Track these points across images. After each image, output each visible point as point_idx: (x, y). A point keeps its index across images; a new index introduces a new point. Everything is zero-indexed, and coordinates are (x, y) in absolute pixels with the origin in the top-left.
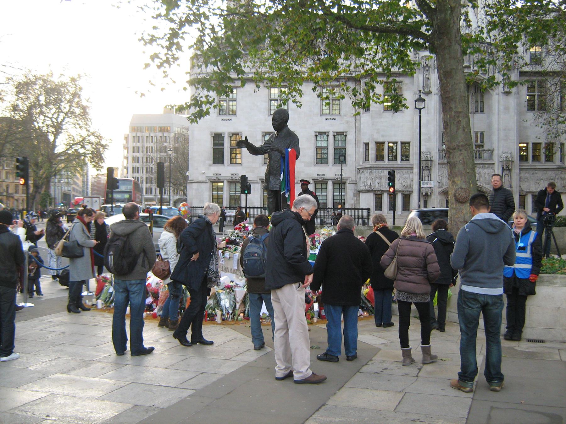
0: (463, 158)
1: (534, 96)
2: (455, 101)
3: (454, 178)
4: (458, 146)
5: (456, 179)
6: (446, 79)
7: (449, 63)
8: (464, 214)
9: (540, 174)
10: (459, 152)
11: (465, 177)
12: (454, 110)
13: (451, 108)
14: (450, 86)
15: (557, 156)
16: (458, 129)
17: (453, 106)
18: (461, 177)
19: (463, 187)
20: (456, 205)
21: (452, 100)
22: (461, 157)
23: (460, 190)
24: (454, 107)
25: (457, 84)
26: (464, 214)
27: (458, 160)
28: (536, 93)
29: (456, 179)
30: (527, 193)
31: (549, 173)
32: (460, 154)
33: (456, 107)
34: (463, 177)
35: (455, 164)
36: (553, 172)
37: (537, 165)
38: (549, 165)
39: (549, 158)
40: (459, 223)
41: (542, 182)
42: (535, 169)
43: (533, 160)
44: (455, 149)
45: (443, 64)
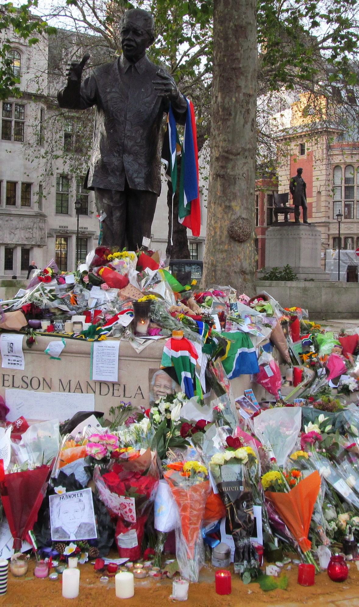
0: (248, 170)
1: (11, 122)
2: (246, 77)
3: (230, 201)
4: (244, 150)
5: (233, 204)
6: (237, 39)
7: (245, 13)
8: (240, 261)
9: (15, 222)
10: (244, 161)
11: (247, 200)
12: (244, 91)
13: (238, 87)
14: (242, 52)
15: (34, 198)
16: (246, 122)
17: (242, 83)
18: (242, 201)
19: (244, 216)
20: (229, 244)
21: (242, 74)
22: (245, 169)
23: (241, 221)
24: (243, 86)
25: (251, 49)
26: (240, 261)
27: (241, 173)
28: (13, 119)
29: (233, 204)
30: (17, 245)
31: (27, 220)
32: (245, 163)
33: (246, 86)
34: (244, 201)
35: (235, 179)
36: (31, 219)
37: (12, 210)
38: (25, 211)
39: (26, 201)
40: (233, 274)
41: (17, 232)
42: (10, 215)
43: (8, 203)
44: (239, 154)
45: (235, 13)
